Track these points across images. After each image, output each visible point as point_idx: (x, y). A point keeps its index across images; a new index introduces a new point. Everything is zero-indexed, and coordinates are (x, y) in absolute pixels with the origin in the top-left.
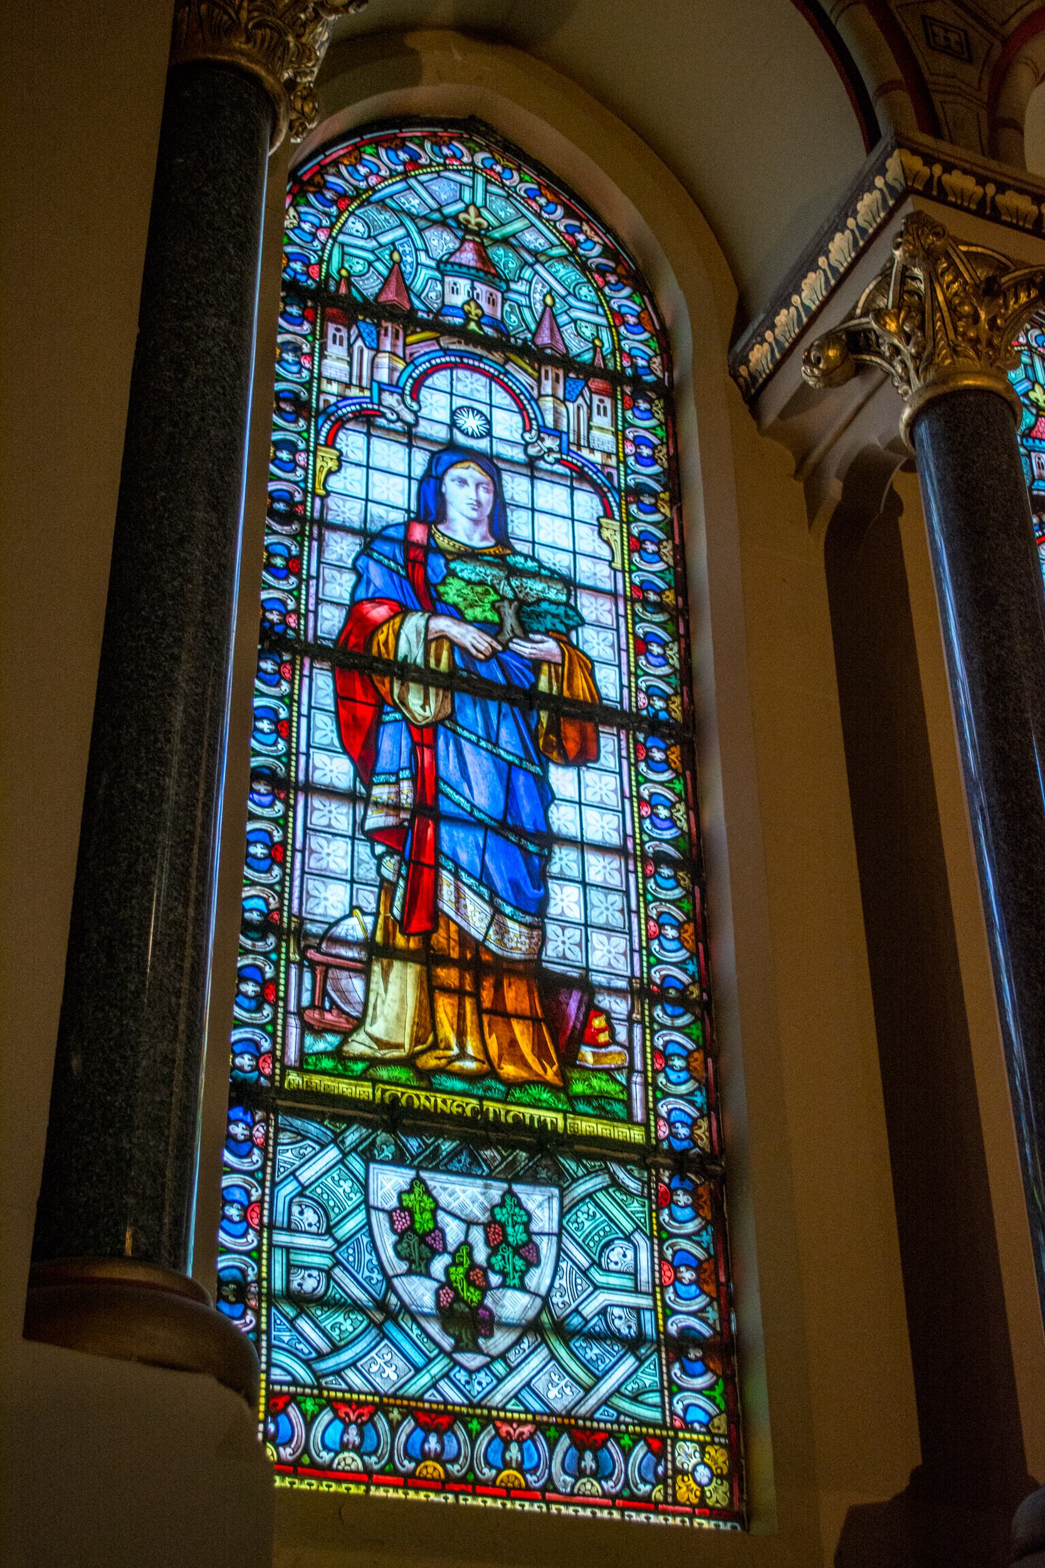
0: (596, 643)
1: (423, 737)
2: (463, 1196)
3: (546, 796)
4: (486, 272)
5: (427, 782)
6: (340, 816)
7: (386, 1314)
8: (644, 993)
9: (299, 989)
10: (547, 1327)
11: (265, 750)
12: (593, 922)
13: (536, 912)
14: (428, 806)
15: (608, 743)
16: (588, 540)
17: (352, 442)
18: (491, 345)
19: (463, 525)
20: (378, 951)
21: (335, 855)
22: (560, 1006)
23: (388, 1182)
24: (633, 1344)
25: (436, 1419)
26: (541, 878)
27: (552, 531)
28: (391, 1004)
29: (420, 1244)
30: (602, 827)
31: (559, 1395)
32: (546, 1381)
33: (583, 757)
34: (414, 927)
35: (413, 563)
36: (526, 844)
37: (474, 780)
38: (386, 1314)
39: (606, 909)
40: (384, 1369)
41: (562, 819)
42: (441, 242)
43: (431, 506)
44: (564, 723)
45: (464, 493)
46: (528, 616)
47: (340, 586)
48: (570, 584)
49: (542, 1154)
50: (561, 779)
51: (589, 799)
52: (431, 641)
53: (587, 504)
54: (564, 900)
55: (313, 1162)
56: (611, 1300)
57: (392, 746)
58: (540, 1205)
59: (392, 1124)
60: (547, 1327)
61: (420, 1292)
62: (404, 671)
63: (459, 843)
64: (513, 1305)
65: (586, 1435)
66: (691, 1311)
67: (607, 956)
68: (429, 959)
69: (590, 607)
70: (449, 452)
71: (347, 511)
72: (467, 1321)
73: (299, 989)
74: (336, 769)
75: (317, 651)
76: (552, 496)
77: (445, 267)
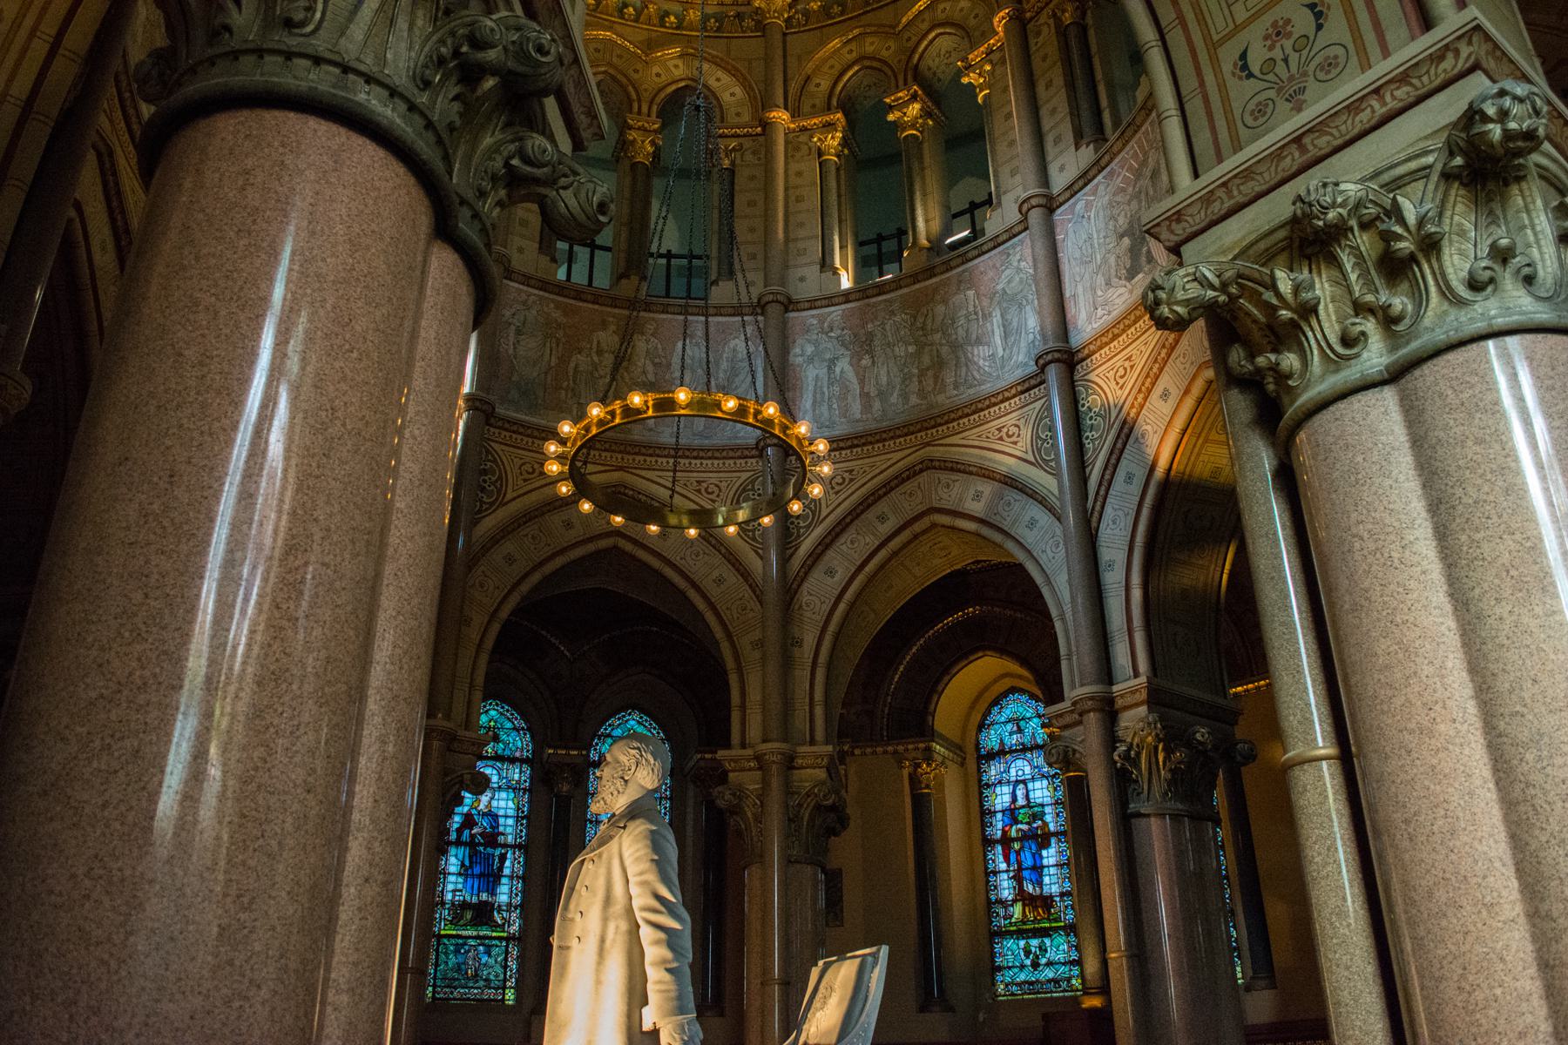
0: (1048, 818)
1: (1018, 853)
2: (1034, 942)
3: (1041, 857)
4: (1020, 730)
5: (1019, 863)
6: (1005, 876)
7: (1022, 967)
8: (1062, 895)
9: (1002, 912)
10: (1050, 964)
11: (991, 866)
12: (1052, 883)
13: (1040, 884)
14: (1020, 869)
15: (1053, 840)
16: (1046, 793)
17: (998, 790)
18: (1025, 749)
19: (1021, 801)
20: (1014, 901)
21: (1005, 884)
22: (1047, 902)
23: (1022, 943)
24: (1064, 964)
25: (1032, 983)
26: (1041, 875)
27: (1038, 794)
28: (1017, 911)
29: (1027, 953)
30: (1052, 861)
31: (1051, 975)
32: (1050, 973)
33: (1046, 845)
34: (1021, 896)
35: (1012, 813)
36: (1038, 869)
37: (1028, 861)
38: (1022, 967)
39: (1054, 879)
40: (1022, 977)
41: (1045, 862)
42: (1009, 727)
43: (1014, 799)
44: (1043, 840)
45: (1020, 793)
46: (1034, 817)
47: (1000, 825)
48: (1042, 805)
49: (1045, 933)
50: (1044, 853)
51: (1050, 856)
52: (1018, 831)
53: (1045, 782)
54: (1046, 880)
55: (1010, 943)
56: (1061, 957)
57: (1013, 858)
58: (1047, 941)
59: (1021, 933)
60: (1050, 964)
61: (1028, 962)
62: (1014, 840)
63: (1026, 874)
64: (1043, 961)
65: (1056, 981)
66: (1074, 956)
67: (1055, 889)
68: (1023, 900)
69: (1048, 810)
70: (1017, 782)
71: (999, 807)
72: (1035, 965)
73: (1002, 912)
74: (1003, 866)
75: (997, 841)
76: (1038, 784)
77: (1011, 734)
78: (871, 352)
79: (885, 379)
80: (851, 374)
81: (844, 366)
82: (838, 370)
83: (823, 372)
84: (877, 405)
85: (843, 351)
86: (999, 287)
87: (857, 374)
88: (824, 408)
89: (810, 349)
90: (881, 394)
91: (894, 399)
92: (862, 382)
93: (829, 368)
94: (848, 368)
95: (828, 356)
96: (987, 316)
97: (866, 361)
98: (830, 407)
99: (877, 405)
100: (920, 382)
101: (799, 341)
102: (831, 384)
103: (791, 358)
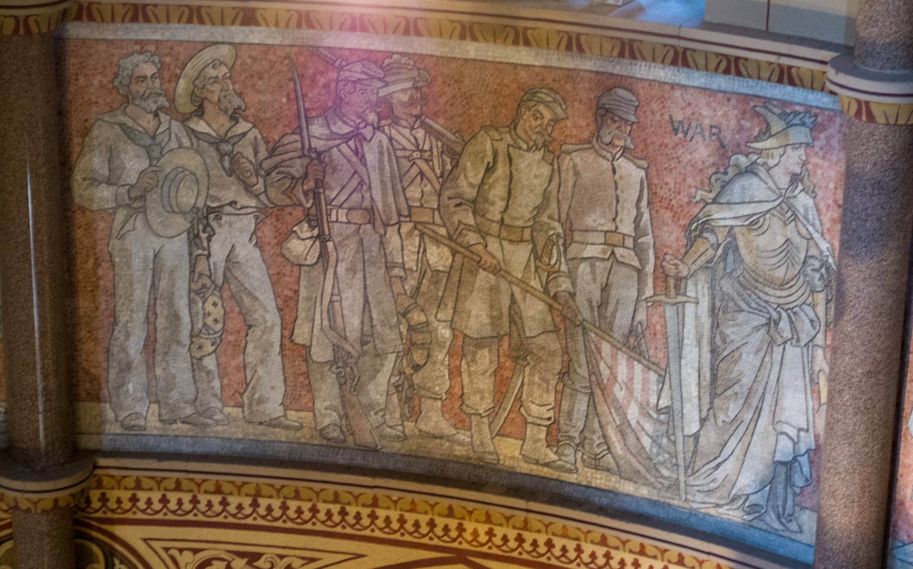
78: (315, 219)
79: (353, 323)
80: (255, 272)
81: (235, 238)
82: (218, 251)
83: (176, 249)
84: (327, 393)
85: (231, 192)
86: (722, 216)
87: (276, 281)
88: (180, 366)
89: (134, 164)
90: (340, 359)
91: (378, 389)
92: (288, 306)
93: (194, 239)
94: (247, 253)
95: (188, 197)
96: (671, 283)
97: (301, 246)
98: (196, 364)
99: (327, 393)
100: (455, 372)
101: (102, 132)
102: (197, 293)
103: (80, 190)
